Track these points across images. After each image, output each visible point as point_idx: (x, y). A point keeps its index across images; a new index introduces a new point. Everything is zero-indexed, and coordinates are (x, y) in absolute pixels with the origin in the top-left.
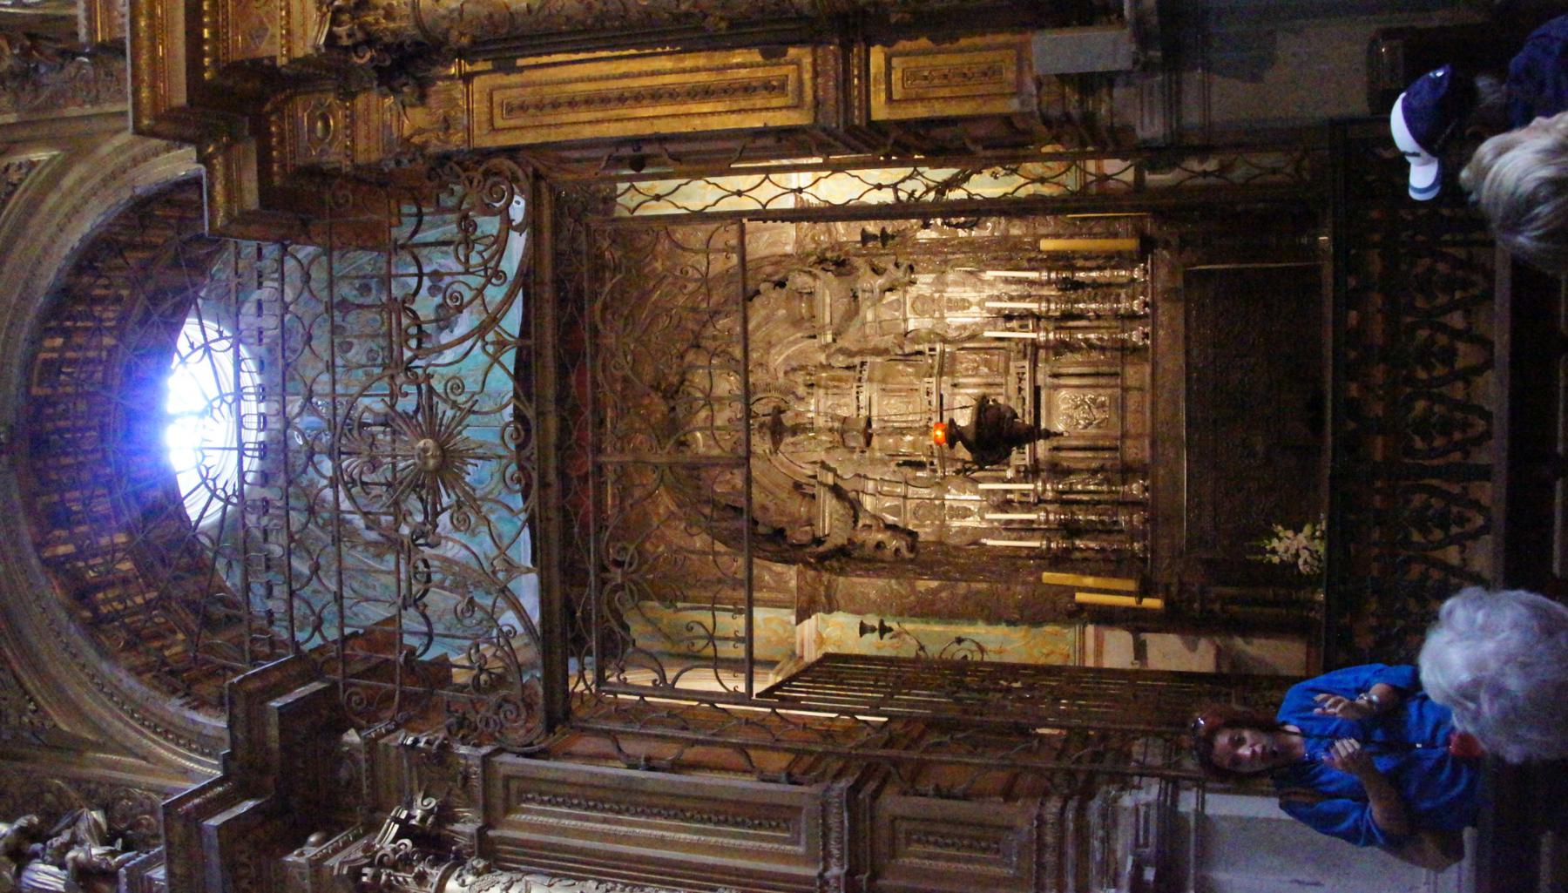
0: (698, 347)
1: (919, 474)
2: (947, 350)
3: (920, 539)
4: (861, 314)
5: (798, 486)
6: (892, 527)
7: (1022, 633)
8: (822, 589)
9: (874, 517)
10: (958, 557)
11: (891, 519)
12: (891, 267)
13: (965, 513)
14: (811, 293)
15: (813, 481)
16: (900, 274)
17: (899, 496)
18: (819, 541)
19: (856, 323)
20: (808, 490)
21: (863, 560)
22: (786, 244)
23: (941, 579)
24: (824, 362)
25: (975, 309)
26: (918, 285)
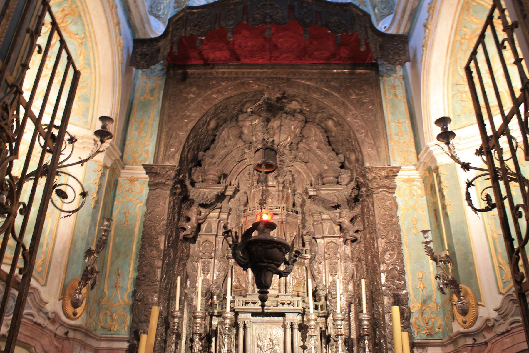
2: (306, 261)
3: (191, 245)
4: (327, 212)
5: (225, 176)
7: (127, 301)
8: (164, 180)
9: (205, 218)
10: (179, 266)
11: (204, 227)
12: (356, 228)
13: (205, 271)
14: (338, 183)
15: (228, 183)
16: (352, 233)
17: (217, 232)
18: (193, 184)
19: (320, 209)
21: (180, 208)
22: (370, 163)
23: (165, 251)
25: (331, 279)
26: (344, 246)
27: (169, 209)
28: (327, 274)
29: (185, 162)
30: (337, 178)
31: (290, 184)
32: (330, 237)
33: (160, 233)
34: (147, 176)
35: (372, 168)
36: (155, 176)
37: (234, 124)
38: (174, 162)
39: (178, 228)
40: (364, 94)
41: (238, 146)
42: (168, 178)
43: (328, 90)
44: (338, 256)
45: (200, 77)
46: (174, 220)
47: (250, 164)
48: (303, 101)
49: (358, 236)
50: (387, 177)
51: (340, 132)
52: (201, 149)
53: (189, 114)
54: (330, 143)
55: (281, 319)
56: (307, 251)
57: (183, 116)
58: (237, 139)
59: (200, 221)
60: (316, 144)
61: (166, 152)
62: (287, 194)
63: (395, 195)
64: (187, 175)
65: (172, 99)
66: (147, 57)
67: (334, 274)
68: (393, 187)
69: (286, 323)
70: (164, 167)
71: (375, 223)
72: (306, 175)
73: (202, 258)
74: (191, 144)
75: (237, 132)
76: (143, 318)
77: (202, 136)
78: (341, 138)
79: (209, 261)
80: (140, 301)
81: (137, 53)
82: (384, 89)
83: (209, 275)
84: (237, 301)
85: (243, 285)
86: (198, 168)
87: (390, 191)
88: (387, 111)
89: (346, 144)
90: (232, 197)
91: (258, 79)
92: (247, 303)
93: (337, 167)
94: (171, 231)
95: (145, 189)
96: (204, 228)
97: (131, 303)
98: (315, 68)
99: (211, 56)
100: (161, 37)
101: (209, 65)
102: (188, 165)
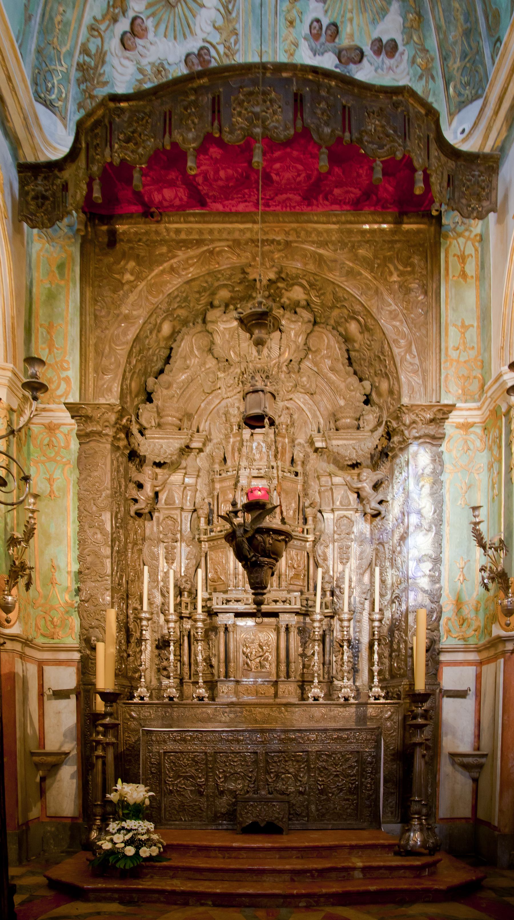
0: (315, 323)
1: (203, 520)
2: (308, 544)
14: (358, 428)
20: (186, 424)
24: (296, 442)
25: (340, 567)
31: (287, 430)
33: (101, 509)
35: (412, 406)
36: (86, 421)
38: (113, 399)
39: (126, 500)
40: (413, 272)
41: (207, 367)
42: (107, 424)
43: (354, 266)
44: (353, 536)
46: (120, 487)
47: (226, 396)
51: (368, 343)
56: (310, 531)
58: (205, 354)
60: (328, 362)
62: (282, 447)
65: (96, 283)
66: (47, 202)
67: (344, 561)
70: (98, 407)
72: (311, 414)
74: (135, 366)
75: (205, 343)
77: (151, 351)
78: (368, 353)
81: (27, 193)
82: (447, 262)
89: (376, 364)
91: (237, 243)
93: (359, 401)
98: (334, 219)
101: (152, 215)
102: (132, 401)
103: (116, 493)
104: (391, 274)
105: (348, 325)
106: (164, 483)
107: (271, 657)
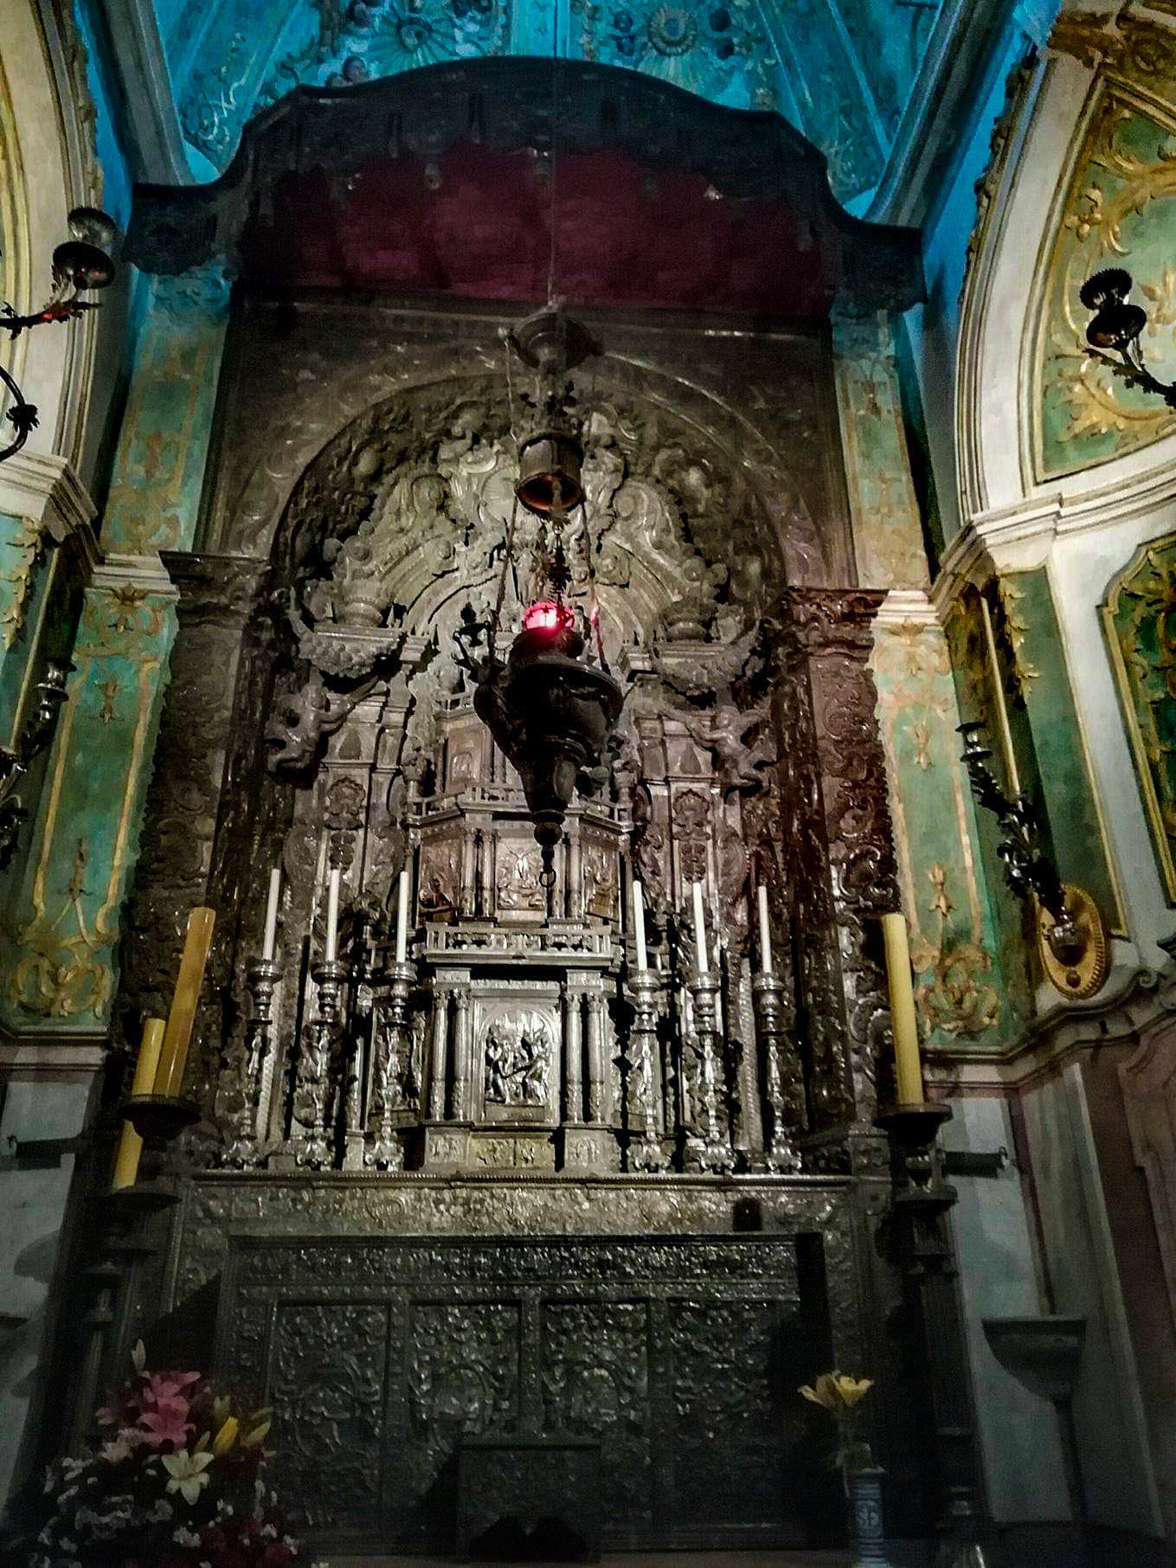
0: (626, 475)
2: (623, 838)
3: (298, 792)
4: (677, 713)
6: (321, 745)
8: (224, 600)
10: (261, 845)
11: (338, 742)
12: (758, 755)
16: (745, 768)
21: (270, 686)
23: (224, 792)
27: (238, 681)
28: (677, 876)
29: (287, 559)
30: (707, 625)
32: (685, 780)
34: (173, 588)
37: (426, 468)
45: (332, 327)
46: (253, 713)
48: (622, 411)
49: (763, 776)
50: (848, 617)
52: (333, 531)
53: (298, 424)
54: (687, 535)
55: (553, 986)
57: (283, 429)
59: (327, 727)
61: (230, 524)
63: (867, 666)
64: (293, 593)
68: (864, 642)
69: (568, 997)
71: (815, 738)
73: (329, 827)
75: (434, 494)
76: (154, 978)
79: (352, 835)
80: (144, 930)
83: (350, 873)
84: (430, 935)
85: (449, 896)
86: (323, 583)
87: (856, 654)
88: (851, 448)
90: (421, 666)
92: (458, 944)
94: (245, 741)
95: (167, 623)
96: (338, 747)
97: (116, 937)
99: (366, 264)
100: (219, 182)
102: (294, 568)
103: (242, 719)
104: (754, 399)
105: (684, 474)
106: (342, 718)
107: (550, 1071)
